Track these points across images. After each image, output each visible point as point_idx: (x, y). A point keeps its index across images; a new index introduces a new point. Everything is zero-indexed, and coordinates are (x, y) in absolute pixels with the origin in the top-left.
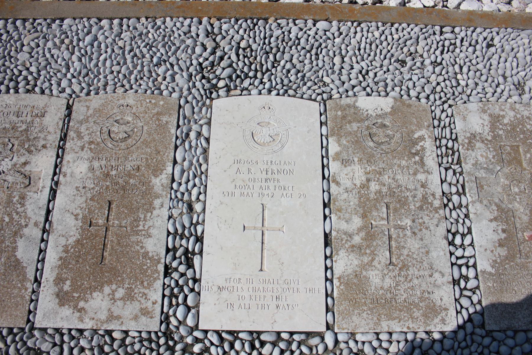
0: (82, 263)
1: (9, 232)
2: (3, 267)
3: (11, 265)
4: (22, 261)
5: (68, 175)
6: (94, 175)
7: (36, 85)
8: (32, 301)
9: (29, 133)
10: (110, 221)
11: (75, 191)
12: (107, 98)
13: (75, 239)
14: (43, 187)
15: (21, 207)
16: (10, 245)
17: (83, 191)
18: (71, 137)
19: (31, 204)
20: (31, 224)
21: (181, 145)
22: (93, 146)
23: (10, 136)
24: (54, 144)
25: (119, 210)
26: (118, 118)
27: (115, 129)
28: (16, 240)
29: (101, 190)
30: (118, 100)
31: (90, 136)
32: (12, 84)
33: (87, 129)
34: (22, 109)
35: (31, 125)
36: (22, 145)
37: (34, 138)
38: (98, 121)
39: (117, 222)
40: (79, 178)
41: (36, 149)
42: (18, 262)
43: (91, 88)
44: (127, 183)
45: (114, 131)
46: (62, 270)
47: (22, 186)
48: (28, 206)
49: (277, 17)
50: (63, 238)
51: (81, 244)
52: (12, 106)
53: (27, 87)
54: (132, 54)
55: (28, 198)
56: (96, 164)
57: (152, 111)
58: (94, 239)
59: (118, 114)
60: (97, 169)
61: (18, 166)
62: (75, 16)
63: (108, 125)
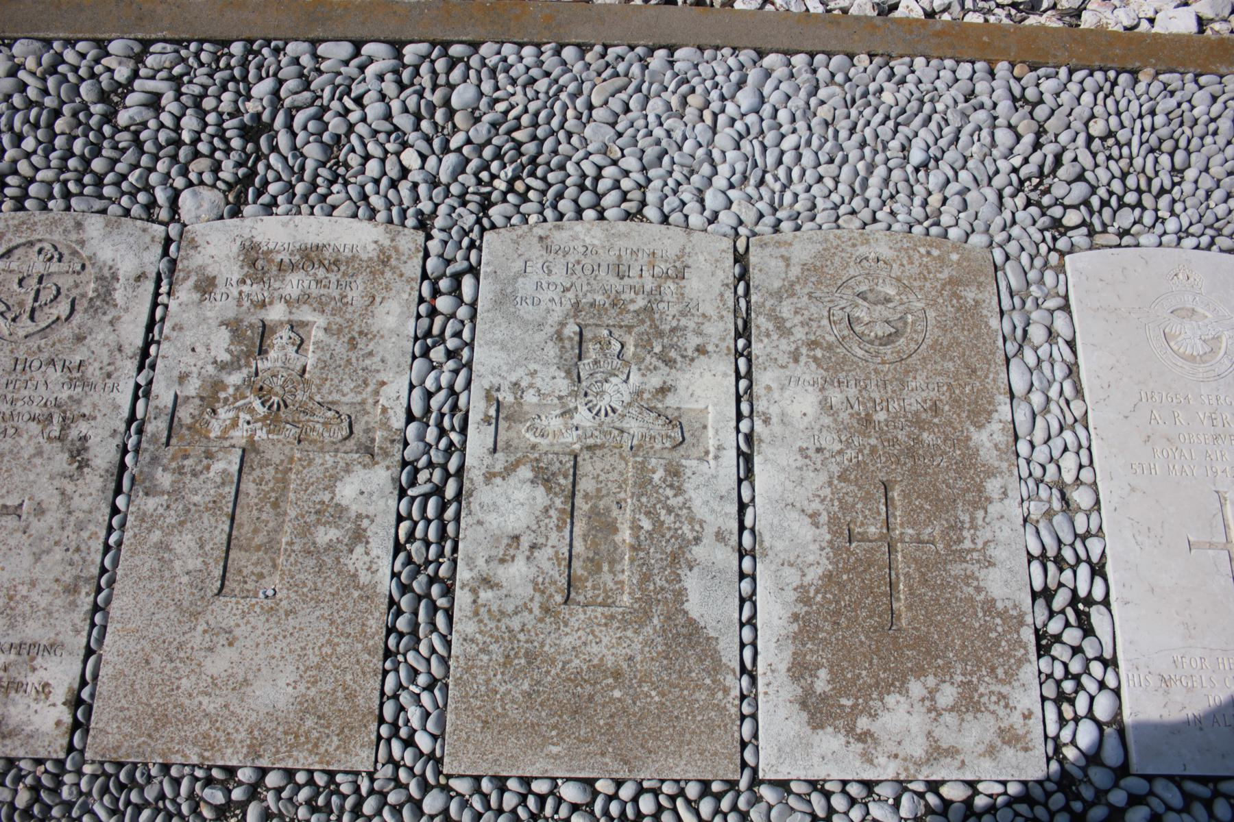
0: (848, 628)
1: (659, 556)
2: (659, 639)
3: (678, 634)
4: (702, 624)
5: (774, 420)
6: (835, 420)
7: (643, 203)
8: (743, 717)
9: (657, 316)
10: (894, 529)
11: (799, 457)
12: (826, 240)
13: (820, 571)
14: (720, 448)
15: (675, 496)
16: (667, 585)
17: (818, 458)
18: (763, 329)
19: (698, 487)
20: (709, 537)
21: (1015, 355)
22: (819, 353)
23: (611, 322)
24: (723, 345)
25: (910, 503)
26: (863, 288)
27: (862, 313)
28: (679, 575)
29: (860, 458)
30: (854, 245)
31: (806, 329)
32: (586, 198)
33: (796, 313)
34: (626, 257)
35: (658, 297)
36: (645, 344)
37: (673, 330)
38: (818, 294)
39: (911, 531)
40: (802, 427)
41: (683, 357)
42: (694, 628)
43: (779, 215)
44: (917, 440)
45: (858, 318)
46: (804, 645)
47: (668, 445)
48: (691, 493)
49: (1159, 67)
50: (793, 570)
51: (838, 583)
52: (600, 251)
53: (625, 206)
54: (856, 138)
55: (689, 473)
56: (836, 397)
57: (938, 275)
58: (865, 571)
59: (859, 278)
60: (839, 406)
61: (646, 396)
62: (702, 42)
63: (843, 303)
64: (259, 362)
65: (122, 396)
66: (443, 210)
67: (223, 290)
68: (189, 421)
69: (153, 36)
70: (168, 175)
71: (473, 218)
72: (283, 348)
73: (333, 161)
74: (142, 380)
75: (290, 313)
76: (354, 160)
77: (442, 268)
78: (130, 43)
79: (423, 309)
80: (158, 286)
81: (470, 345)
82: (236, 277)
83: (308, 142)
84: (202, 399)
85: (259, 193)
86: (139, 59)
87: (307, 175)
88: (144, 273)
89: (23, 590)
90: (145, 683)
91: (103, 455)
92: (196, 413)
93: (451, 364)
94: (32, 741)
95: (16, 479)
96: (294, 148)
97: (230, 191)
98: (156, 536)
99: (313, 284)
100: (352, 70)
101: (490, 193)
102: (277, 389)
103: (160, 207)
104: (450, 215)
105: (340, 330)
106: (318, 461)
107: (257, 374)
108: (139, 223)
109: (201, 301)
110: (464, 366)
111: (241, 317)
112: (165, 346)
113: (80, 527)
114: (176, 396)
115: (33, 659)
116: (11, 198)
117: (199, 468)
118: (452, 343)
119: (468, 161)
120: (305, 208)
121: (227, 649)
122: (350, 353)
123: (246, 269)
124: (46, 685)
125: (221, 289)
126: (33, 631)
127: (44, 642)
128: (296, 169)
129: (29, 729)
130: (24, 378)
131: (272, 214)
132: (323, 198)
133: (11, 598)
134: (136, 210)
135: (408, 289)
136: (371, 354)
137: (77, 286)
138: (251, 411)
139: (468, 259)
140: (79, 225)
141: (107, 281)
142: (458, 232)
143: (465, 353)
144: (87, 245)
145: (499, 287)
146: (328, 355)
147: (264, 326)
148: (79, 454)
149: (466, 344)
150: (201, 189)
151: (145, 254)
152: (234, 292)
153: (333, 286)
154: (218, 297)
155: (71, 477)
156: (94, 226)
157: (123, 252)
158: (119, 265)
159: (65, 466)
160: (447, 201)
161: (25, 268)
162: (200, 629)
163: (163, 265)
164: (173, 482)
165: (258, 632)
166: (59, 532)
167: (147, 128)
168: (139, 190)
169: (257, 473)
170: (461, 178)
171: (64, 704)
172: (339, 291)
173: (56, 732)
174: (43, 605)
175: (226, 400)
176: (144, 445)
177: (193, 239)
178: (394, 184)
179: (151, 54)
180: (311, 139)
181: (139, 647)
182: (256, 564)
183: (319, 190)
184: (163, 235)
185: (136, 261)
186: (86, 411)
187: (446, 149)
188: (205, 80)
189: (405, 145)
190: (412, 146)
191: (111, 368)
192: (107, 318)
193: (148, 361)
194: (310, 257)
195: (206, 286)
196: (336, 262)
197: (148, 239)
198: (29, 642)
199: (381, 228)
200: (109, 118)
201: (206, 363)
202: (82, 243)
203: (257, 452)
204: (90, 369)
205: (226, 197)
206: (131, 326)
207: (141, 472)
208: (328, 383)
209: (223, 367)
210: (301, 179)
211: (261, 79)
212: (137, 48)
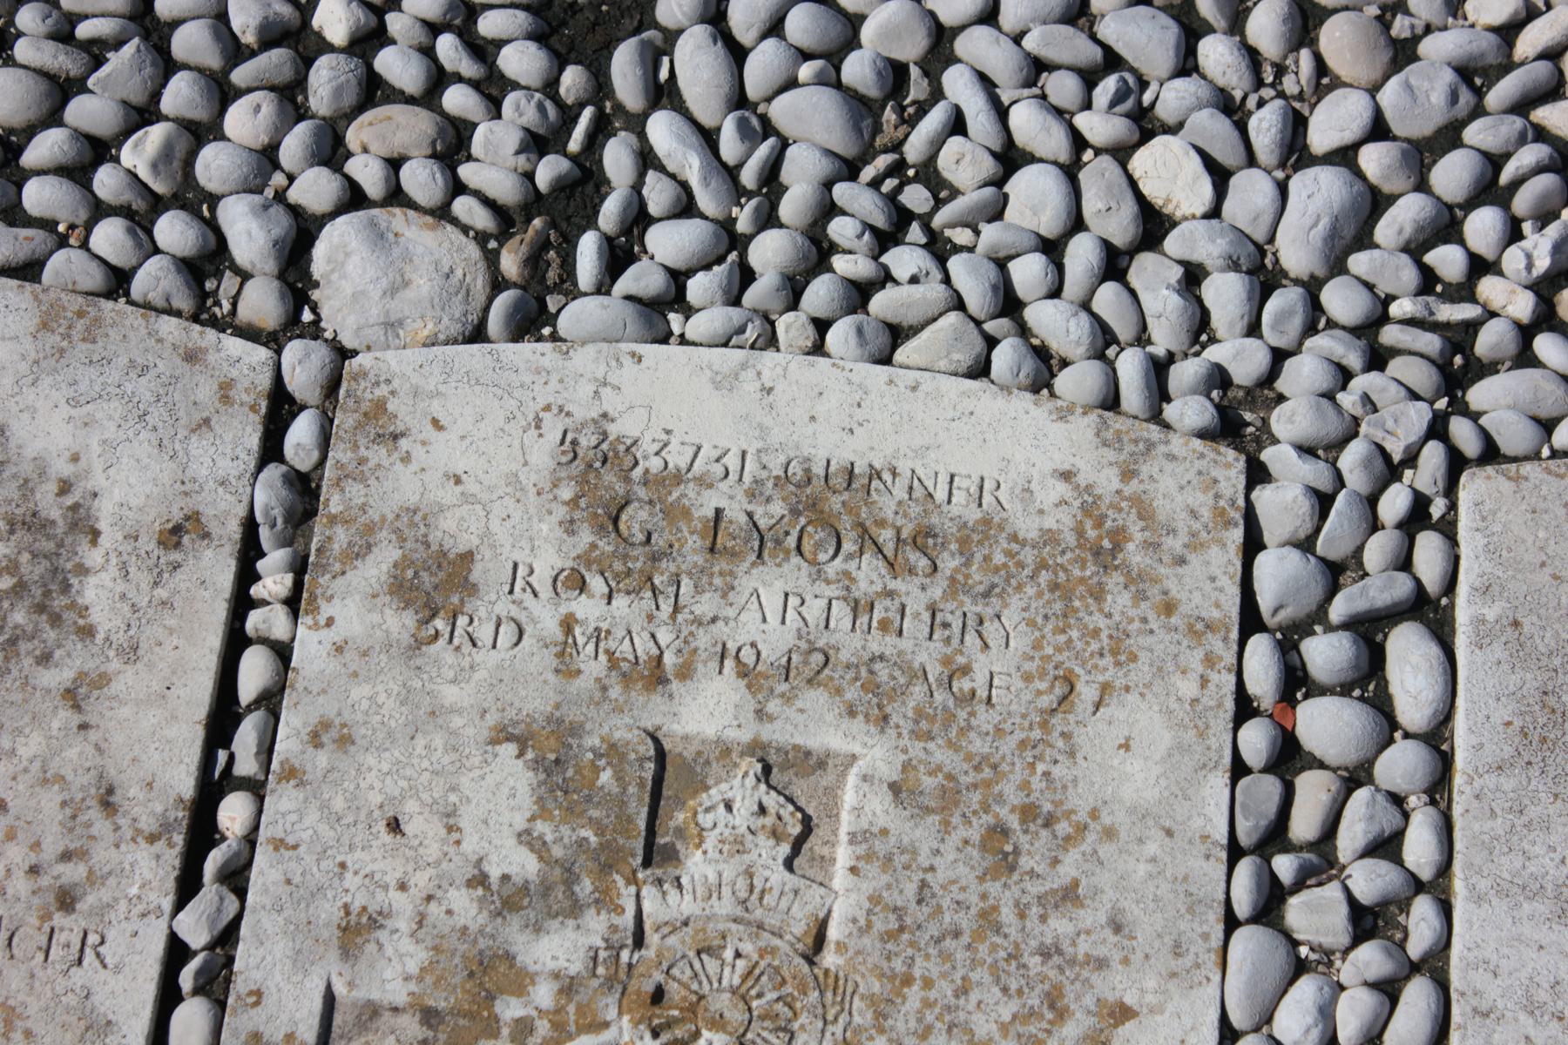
64: (649, 892)
65: (115, 983)
66: (1303, 374)
67: (504, 607)
70: (268, 156)
71: (1418, 417)
72: (739, 846)
74: (195, 927)
75: (760, 714)
77: (1316, 591)
79: (1256, 740)
80: (247, 574)
81: (1438, 887)
82: (547, 562)
83: (791, 84)
84: (429, 1016)
85: (618, 257)
87: (794, 205)
88: (194, 517)
93: (1371, 959)
96: (739, 100)
97: (504, 235)
99: (841, 612)
101: (1471, 328)
102: (722, 1002)
103: (245, 276)
104: (1329, 396)
105: (950, 796)
107: (639, 940)
108: (168, 325)
109: (419, 643)
110: (1415, 968)
111: (572, 714)
112: (282, 800)
114: (330, 1000)
118: (1369, 880)
119: (1377, 202)
120: (791, 327)
122: (994, 888)
123: (586, 537)
125: (490, 605)
128: (748, 177)
131: (664, 338)
132: (859, 294)
134: (152, 278)
135: (1195, 660)
136: (1069, 895)
139: (1405, 563)
142: (1367, 463)
143: (1421, 921)
145: (1532, 681)
146: (911, 889)
147: (661, 756)
149: (1419, 886)
150: (397, 218)
151: (199, 447)
152: (545, 617)
154: (484, 633)
157: (111, 431)
158: (98, 480)
160: (1322, 342)
163: (269, 494)
168: (158, 204)
170: (1360, 262)
172: (937, 646)
177: (380, 406)
178: (1114, 265)
180: (806, 71)
183: (840, 263)
184: (265, 381)
185: (165, 471)
187: (1295, 152)
189: (1146, 125)
190: (1174, 129)
191: (73, 872)
192: (55, 678)
193: (213, 862)
196: (923, 539)
197: (206, 392)
199: (1084, 426)
201: (443, 882)
205: (492, 259)
206: (151, 718)
208: (914, 994)
210: (768, 219)
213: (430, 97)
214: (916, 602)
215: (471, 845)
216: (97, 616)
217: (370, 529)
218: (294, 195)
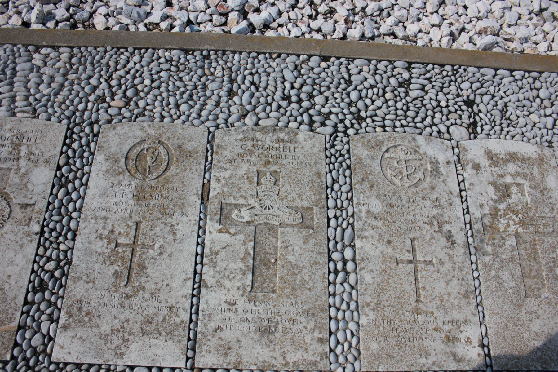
68: (489, 224)
69: (413, 61)
73: (504, 118)
76: (513, 117)
78: (405, 63)
83: (493, 110)
86: (409, 68)
87: (498, 122)
89: (446, 297)
90: (509, 336)
91: (460, 239)
92: (491, 221)
94: (471, 363)
95: (427, 249)
97: (468, 128)
98: (493, 273)
100: (497, 79)
102: (520, 211)
103: (443, 133)
106: (546, 241)
111: (495, 181)
113: (461, 270)
115: (459, 327)
116: (379, 126)
117: (501, 244)
121: (537, 320)
123: (490, 161)
124: (468, 338)
125: (483, 169)
126: (456, 315)
127: (462, 320)
129: (467, 358)
130: (415, 205)
132: (508, 132)
133: (442, 301)
136: (550, 197)
137: (422, 165)
138: (513, 220)
140: (414, 139)
141: (435, 164)
144: (421, 148)
148: (450, 238)
150: (457, 126)
151: (447, 153)
152: (489, 170)
153: (526, 169)
155: (450, 248)
156: (421, 140)
158: (437, 157)
159: (446, 243)
161: (398, 157)
162: (524, 311)
163: (456, 158)
164: (492, 250)
165: (547, 313)
166: (453, 272)
167: (425, 99)
169: (523, 246)
171: (479, 346)
173: (479, 359)
174: (456, 304)
175: (501, 215)
176: (475, 234)
179: (413, 68)
181: (501, 320)
182: (536, 284)
186: (447, 219)
188: (441, 80)
190: (533, 113)
191: (450, 201)
192: (441, 180)
194: (513, 157)
195: (477, 167)
197: (445, 147)
198: (455, 320)
200: (407, 93)
202: (418, 147)
203: (520, 237)
204: (442, 202)
205: (468, 130)
206: (453, 183)
207: (478, 246)
209: (496, 201)
211: (463, 82)
212: (407, 65)
213: (456, 112)
214: (525, 166)
215: (490, 196)
216: (443, 172)
217: (468, 161)
218: (445, 123)
